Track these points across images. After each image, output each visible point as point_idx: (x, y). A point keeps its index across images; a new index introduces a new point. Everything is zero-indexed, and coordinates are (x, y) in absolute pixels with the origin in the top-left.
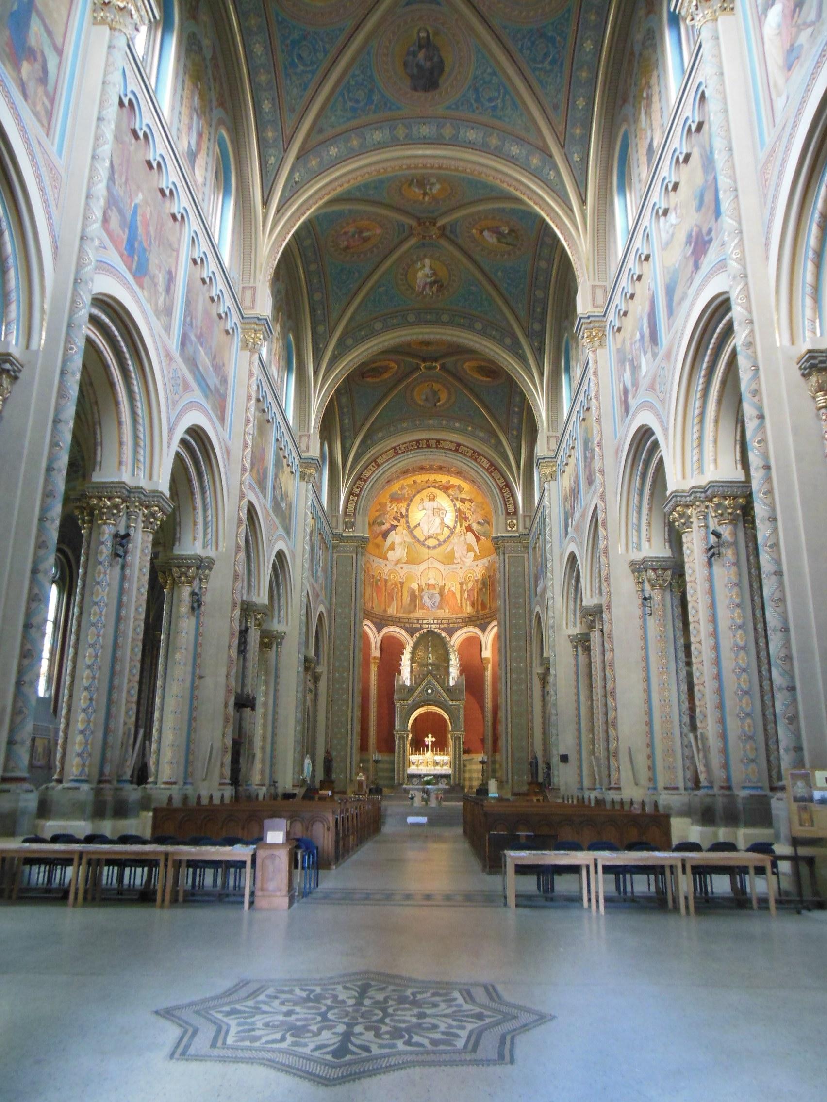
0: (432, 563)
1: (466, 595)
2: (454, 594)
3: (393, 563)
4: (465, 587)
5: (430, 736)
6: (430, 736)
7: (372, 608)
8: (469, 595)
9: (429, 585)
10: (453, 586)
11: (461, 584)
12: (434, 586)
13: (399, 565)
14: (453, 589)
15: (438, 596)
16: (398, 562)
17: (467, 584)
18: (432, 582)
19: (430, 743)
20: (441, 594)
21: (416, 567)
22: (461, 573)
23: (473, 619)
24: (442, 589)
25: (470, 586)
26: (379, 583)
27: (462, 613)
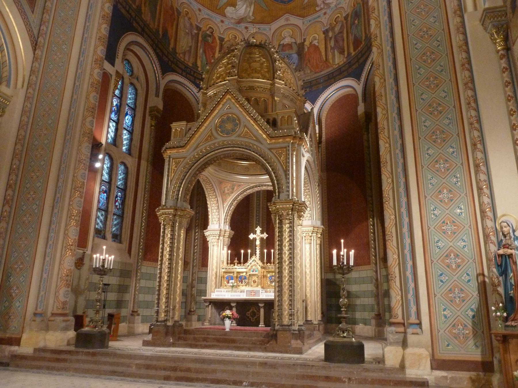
0: (287, 20)
1: (332, 43)
2: (317, 48)
3: (233, 21)
4: (330, 34)
5: (258, 229)
6: (258, 229)
7: (195, 64)
8: (336, 41)
9: (284, 45)
10: (315, 37)
11: (326, 32)
12: (290, 46)
13: (243, 25)
14: (315, 42)
15: (295, 56)
16: (240, 21)
17: (332, 28)
18: (287, 40)
19: (258, 243)
20: (300, 53)
21: (266, 27)
22: (325, 20)
23: (344, 69)
24: (301, 46)
25: (337, 29)
26: (210, 40)
27: (328, 67)
